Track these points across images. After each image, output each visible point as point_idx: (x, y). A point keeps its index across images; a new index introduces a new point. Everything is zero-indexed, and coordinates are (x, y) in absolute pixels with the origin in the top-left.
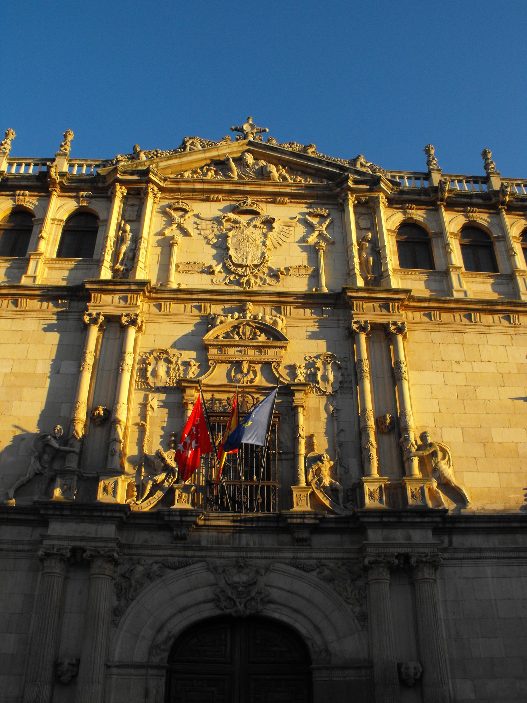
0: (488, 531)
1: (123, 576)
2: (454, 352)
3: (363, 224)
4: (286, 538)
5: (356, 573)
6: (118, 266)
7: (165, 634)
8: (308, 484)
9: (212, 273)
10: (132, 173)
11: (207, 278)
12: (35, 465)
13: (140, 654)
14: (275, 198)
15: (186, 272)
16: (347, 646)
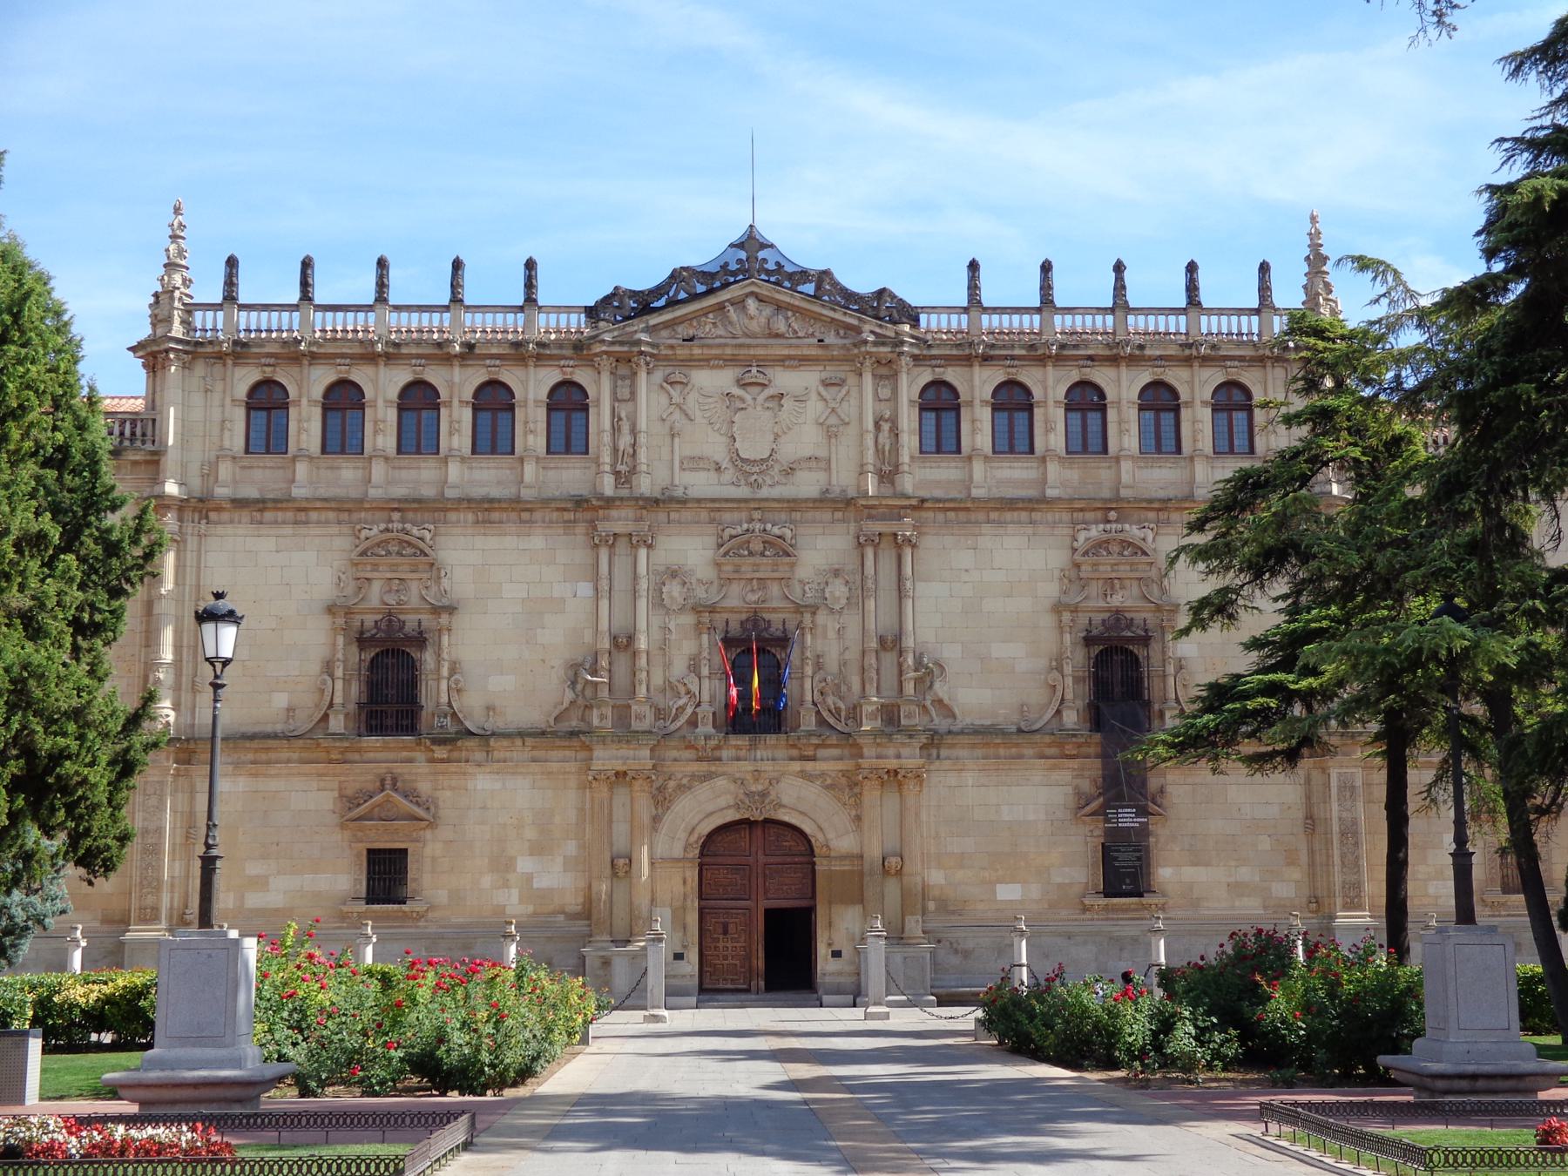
0: (973, 746)
1: (658, 789)
2: (964, 558)
3: (885, 392)
4: (795, 752)
5: (850, 786)
6: (620, 467)
7: (696, 835)
8: (814, 704)
9: (718, 469)
10: (622, 343)
11: (713, 475)
12: (569, 695)
13: (678, 852)
14: (782, 361)
15: (692, 469)
16: (844, 843)
